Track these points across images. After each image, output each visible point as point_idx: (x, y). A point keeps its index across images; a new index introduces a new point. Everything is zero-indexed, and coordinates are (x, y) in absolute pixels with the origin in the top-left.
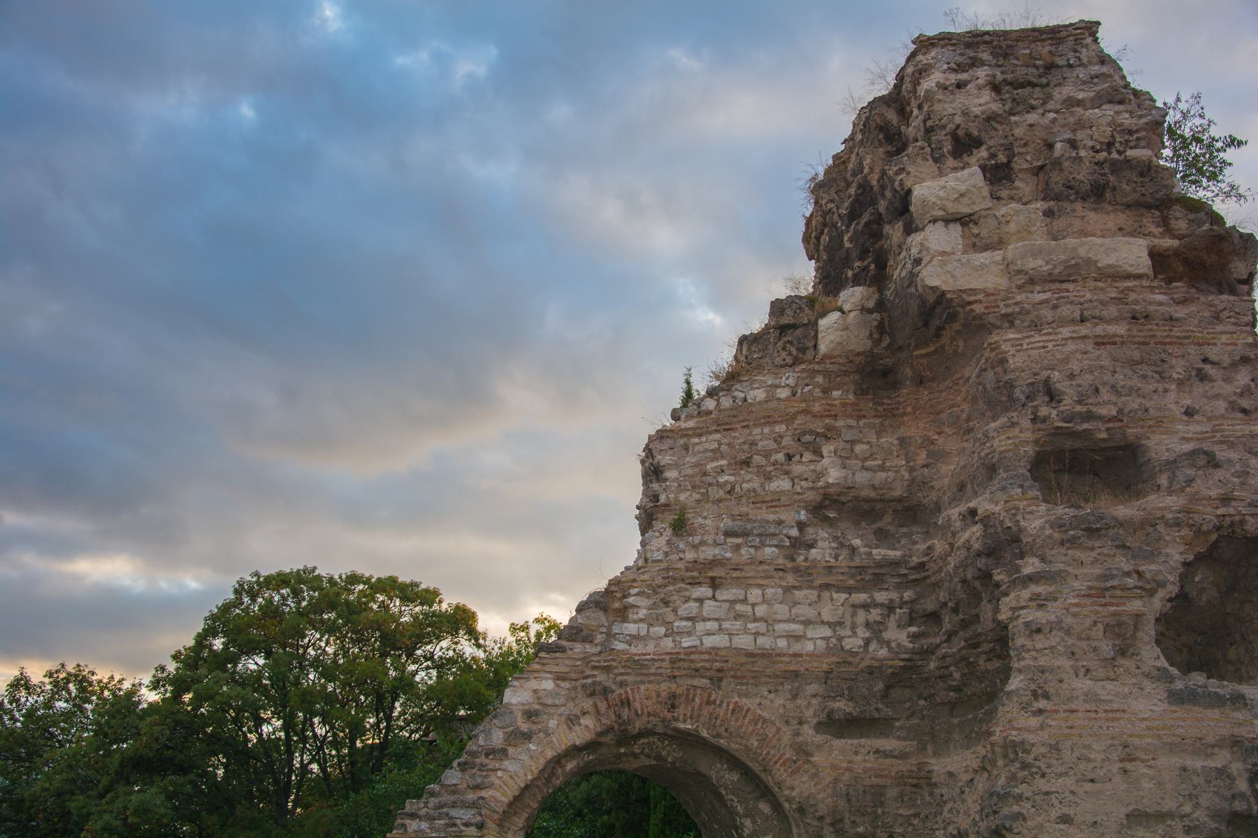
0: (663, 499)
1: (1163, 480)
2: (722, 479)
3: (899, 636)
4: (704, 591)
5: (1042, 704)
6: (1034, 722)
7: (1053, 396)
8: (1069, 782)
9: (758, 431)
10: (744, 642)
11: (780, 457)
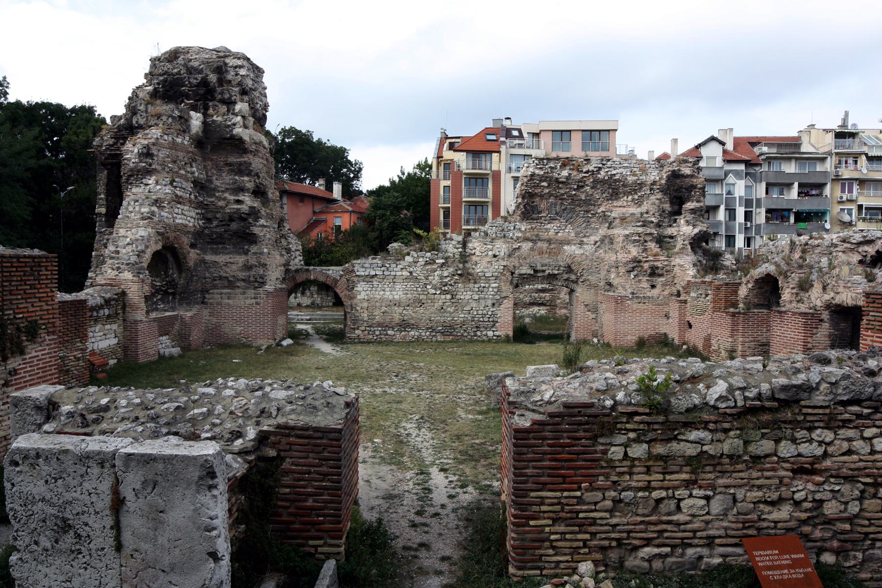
4: (179, 206)
7: (259, 177)
10: (184, 222)
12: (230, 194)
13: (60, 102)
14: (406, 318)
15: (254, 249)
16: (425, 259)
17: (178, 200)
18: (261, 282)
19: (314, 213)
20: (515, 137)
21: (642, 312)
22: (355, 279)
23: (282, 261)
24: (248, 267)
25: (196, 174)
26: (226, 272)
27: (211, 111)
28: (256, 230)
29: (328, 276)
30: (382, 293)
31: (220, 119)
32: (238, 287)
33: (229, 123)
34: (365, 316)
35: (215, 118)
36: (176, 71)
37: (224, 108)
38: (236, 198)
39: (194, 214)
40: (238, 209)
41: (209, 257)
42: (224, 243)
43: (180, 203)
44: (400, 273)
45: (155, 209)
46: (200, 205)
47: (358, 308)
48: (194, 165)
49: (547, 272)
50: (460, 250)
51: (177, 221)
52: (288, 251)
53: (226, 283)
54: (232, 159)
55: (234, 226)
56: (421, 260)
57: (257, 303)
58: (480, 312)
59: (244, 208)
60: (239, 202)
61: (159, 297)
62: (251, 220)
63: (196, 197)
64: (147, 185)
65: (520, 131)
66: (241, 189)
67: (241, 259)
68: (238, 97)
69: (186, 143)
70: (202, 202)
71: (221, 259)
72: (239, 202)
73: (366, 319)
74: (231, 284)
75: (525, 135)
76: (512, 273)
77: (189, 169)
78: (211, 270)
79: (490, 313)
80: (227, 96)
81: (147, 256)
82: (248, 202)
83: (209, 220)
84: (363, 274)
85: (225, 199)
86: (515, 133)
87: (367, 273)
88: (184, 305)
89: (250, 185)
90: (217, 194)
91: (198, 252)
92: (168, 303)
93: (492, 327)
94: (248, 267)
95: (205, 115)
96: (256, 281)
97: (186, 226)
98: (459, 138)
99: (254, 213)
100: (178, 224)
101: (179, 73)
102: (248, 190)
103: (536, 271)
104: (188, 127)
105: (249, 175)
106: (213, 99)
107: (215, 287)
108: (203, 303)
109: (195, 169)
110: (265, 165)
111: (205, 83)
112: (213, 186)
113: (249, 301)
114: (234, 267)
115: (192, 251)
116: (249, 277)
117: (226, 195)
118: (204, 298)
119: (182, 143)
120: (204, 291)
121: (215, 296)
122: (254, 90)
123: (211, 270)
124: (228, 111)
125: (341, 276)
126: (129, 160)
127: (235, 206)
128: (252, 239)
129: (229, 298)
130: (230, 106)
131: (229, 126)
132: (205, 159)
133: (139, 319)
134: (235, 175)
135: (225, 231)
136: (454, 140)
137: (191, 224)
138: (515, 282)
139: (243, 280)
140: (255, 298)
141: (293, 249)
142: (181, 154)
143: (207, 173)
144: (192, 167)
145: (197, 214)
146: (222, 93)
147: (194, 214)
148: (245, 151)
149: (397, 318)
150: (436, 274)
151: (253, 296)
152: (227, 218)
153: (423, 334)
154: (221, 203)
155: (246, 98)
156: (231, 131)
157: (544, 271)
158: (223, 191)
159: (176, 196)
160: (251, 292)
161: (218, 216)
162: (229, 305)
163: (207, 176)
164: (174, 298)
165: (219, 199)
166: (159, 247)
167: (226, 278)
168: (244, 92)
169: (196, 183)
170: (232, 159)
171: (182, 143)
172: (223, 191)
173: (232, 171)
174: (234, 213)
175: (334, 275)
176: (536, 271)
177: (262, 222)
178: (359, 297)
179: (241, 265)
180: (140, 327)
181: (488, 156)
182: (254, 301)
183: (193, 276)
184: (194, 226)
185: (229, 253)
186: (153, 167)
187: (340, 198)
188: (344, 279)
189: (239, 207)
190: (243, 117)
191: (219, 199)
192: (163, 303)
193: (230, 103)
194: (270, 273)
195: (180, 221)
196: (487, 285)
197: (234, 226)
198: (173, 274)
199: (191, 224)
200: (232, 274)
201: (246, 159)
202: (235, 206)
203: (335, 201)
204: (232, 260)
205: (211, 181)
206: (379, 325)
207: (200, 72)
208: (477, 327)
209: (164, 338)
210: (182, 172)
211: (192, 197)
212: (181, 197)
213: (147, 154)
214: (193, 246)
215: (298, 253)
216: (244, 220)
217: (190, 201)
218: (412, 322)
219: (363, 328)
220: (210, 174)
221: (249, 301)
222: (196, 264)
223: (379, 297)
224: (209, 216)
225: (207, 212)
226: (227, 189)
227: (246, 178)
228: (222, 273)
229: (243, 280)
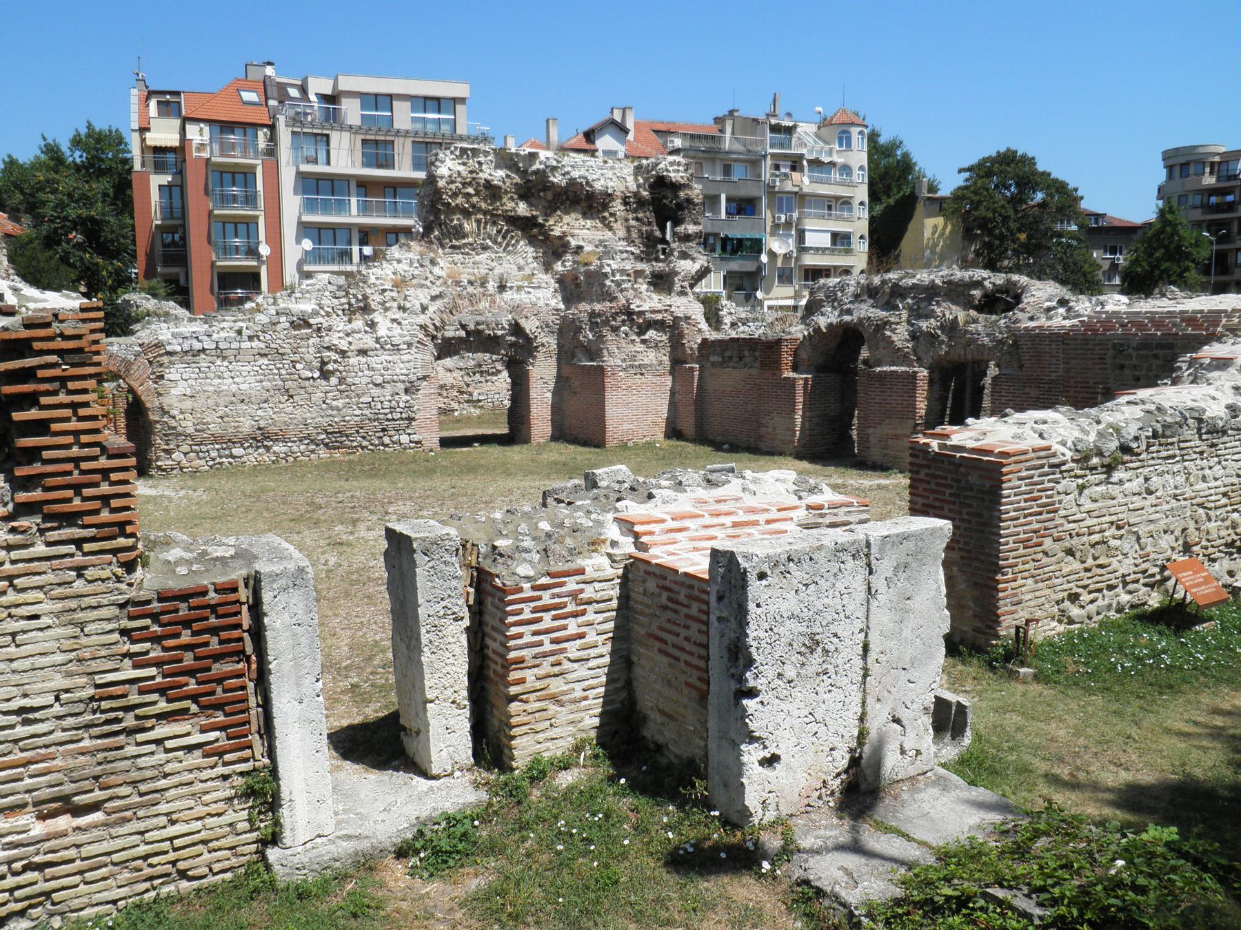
14: (262, 424)
21: (639, 388)
30: (217, 381)
34: (188, 425)
44: (248, 344)
47: (174, 412)
56: (283, 319)
58: (386, 404)
73: (190, 430)
79: (402, 405)
87: (186, 348)
125: (137, 355)
149: (247, 426)
150: (311, 341)
153: (295, 449)
175: (123, 354)
176: (468, 333)
178: (173, 391)
181: (250, 131)
206: (216, 439)
208: (384, 430)
218: (274, 429)
223: (211, 388)
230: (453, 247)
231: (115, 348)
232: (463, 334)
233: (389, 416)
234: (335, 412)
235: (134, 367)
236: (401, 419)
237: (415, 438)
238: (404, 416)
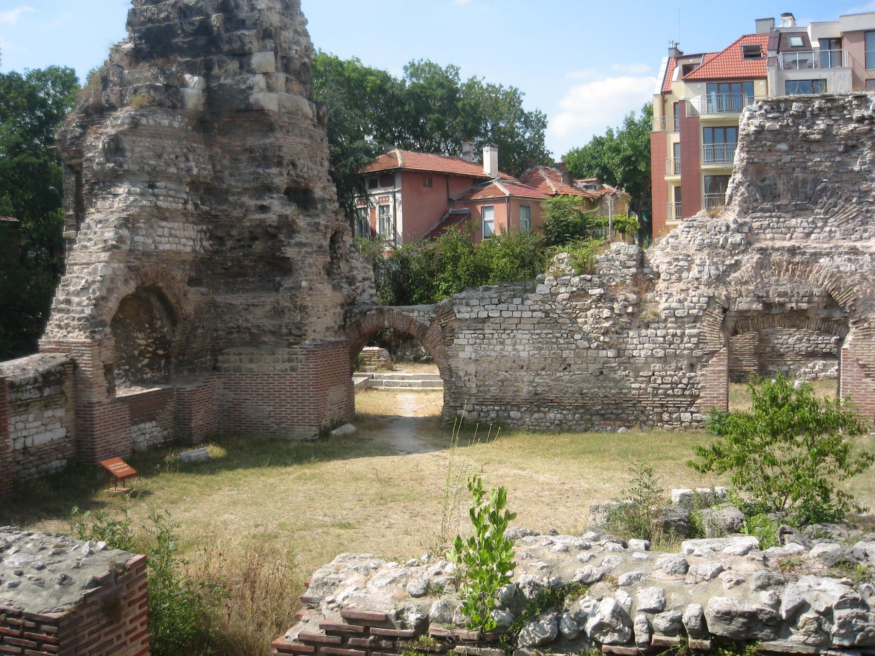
0: (126, 167)
1: (319, 206)
2: (152, 162)
3: (206, 244)
4: (164, 224)
5: (311, 292)
6: (309, 299)
8: (315, 318)
9: (166, 141)
10: (174, 247)
11: (173, 156)
12: (250, 197)
13: (51, 64)
14: (539, 389)
15: (288, 283)
16: (569, 289)
17: (161, 214)
18: (296, 334)
19: (450, 200)
20: (796, 49)
22: (455, 325)
23: (339, 298)
24: (278, 312)
25: (195, 171)
26: (247, 321)
27: (216, 71)
28: (290, 252)
29: (411, 321)
30: (498, 348)
31: (229, 81)
32: (265, 343)
33: (243, 87)
35: (222, 81)
36: (163, 15)
37: (233, 65)
38: (259, 203)
39: (193, 234)
40: (262, 221)
41: (220, 299)
42: (245, 275)
43: (166, 219)
45: (125, 232)
46: (202, 218)
47: (461, 373)
48: (191, 157)
49: (789, 306)
50: (633, 270)
51: (161, 248)
52: (351, 281)
53: (247, 336)
54: (252, 141)
55: (258, 247)
56: (563, 290)
57: (293, 369)
59: (271, 218)
60: (263, 209)
61: (146, 361)
62: (282, 237)
63: (196, 206)
64: (116, 195)
65: (804, 36)
66: (268, 189)
67: (268, 299)
68: (255, 45)
69: (176, 125)
70: (207, 213)
71: (239, 300)
72: (263, 209)
74: (253, 339)
75: (815, 44)
76: (725, 311)
77: (182, 165)
78: (226, 317)
79: (685, 381)
80: (237, 45)
81: (110, 305)
82: (278, 207)
83: (221, 240)
84: (467, 316)
85: (242, 205)
86: (797, 41)
87: (474, 315)
88: (186, 373)
89: (281, 181)
90: (231, 199)
91: (203, 290)
92: (159, 369)
93: (691, 404)
94: (278, 312)
95: (208, 76)
96: (290, 334)
97: (178, 253)
98: (699, 56)
99: (287, 226)
100: (164, 251)
101: (167, 18)
102: (277, 190)
103: (768, 306)
104: (182, 101)
105: (279, 164)
106: (219, 51)
107: (231, 344)
108: (215, 368)
109: (193, 164)
110: (306, 145)
111: (205, 28)
112: (225, 186)
113: (280, 366)
114: (259, 312)
115: (193, 290)
116: (281, 327)
117: (245, 199)
118: (216, 361)
119: (171, 126)
120: (216, 351)
121: (231, 359)
122: (284, 27)
123: (226, 317)
124: (241, 67)
125: (432, 320)
126: (90, 160)
127: (258, 216)
128: (284, 267)
129: (251, 361)
130: (245, 60)
131: (243, 91)
132: (209, 145)
133: (95, 400)
134: (258, 166)
135: (245, 255)
136: (691, 61)
137: (188, 249)
138: (731, 324)
139: (273, 333)
140: (290, 361)
141: (360, 278)
142: (168, 143)
143: (214, 167)
144: (187, 160)
145: (202, 231)
146: (230, 41)
147: (193, 234)
148: (271, 128)
149: (525, 390)
151: (286, 357)
152: (246, 235)
153: (570, 417)
154: (237, 213)
155: (270, 43)
156: (247, 98)
157: (782, 305)
158: (239, 193)
159: (158, 208)
160: (283, 352)
161: (234, 232)
162: (251, 370)
163: (215, 172)
164: (168, 362)
165: (234, 206)
166: (131, 288)
167: (248, 329)
168: (267, 34)
169: (195, 185)
170: (252, 141)
171: (171, 126)
172: (239, 193)
173: (254, 159)
174: (257, 226)
175: (421, 320)
177: (301, 238)
178: (461, 355)
179: (268, 307)
180: (97, 412)
181: (746, 83)
182: (287, 365)
183: (195, 329)
184: (194, 251)
185: (253, 290)
186: (126, 167)
187: (496, 174)
188: (437, 327)
189: (263, 216)
190: (266, 74)
191: (234, 206)
192: (152, 370)
193: (242, 55)
194: (313, 319)
195: (167, 247)
196: (679, 332)
197: (258, 247)
198: (162, 327)
199: (188, 249)
200: (256, 323)
201: (272, 140)
202: (258, 216)
203: (483, 181)
204: (255, 301)
205: (221, 180)
206: (496, 401)
207: (199, 11)
208: (662, 406)
209: (148, 425)
210: (173, 170)
211: (190, 207)
212: (168, 209)
213: (115, 148)
214: (193, 282)
215: (367, 283)
216: (273, 236)
217: (185, 214)
218: (551, 396)
219: (470, 407)
220: (218, 167)
221: (280, 366)
222: (199, 311)
223: (493, 354)
224: (220, 234)
225: (216, 227)
226: (245, 189)
227: (274, 170)
228: (240, 322)
229: (273, 333)
230: (763, 210)
231: (416, 314)
232: (760, 307)
233: (670, 392)
234: (612, 384)
235: (429, 332)
236: (683, 395)
237: (698, 416)
238: (687, 393)
